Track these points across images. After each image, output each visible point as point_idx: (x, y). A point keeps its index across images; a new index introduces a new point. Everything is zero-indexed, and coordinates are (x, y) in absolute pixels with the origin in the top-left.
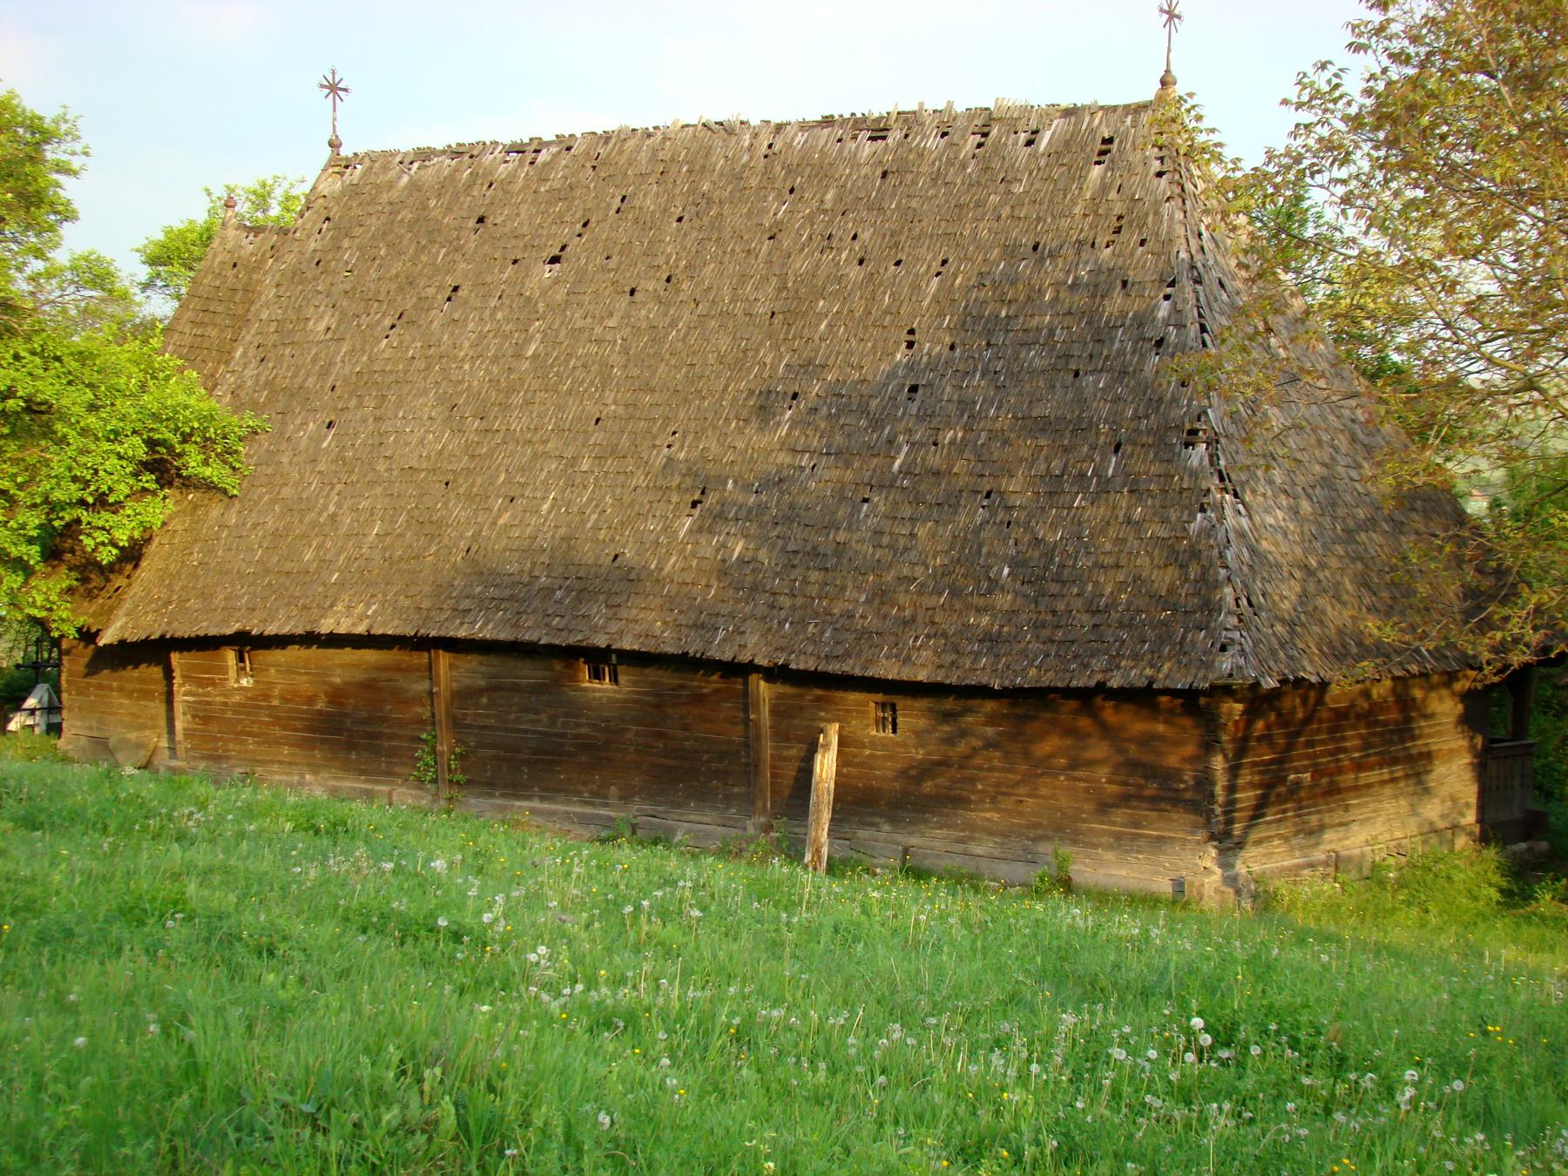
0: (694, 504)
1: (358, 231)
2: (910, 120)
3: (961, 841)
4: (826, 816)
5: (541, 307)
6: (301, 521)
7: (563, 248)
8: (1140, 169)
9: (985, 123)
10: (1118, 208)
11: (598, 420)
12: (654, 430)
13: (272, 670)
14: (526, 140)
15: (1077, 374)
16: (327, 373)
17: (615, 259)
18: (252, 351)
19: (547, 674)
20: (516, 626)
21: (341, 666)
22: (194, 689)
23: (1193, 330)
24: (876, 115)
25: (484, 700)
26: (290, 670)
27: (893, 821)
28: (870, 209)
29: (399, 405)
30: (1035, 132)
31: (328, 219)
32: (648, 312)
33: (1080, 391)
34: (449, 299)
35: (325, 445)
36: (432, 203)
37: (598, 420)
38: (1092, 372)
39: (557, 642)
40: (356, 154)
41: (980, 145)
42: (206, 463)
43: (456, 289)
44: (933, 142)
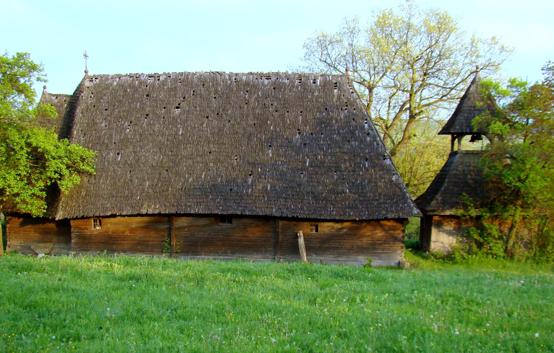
0: (250, 175)
1: (104, 97)
2: (277, 74)
3: (336, 257)
4: (305, 254)
5: (179, 121)
6: (119, 181)
7: (179, 104)
8: (347, 91)
9: (300, 77)
10: (345, 101)
11: (210, 153)
12: (230, 155)
13: (109, 225)
14: (153, 74)
15: (349, 141)
16: (112, 138)
17: (198, 109)
18: (80, 132)
19: (209, 222)
20: (209, 209)
21: (136, 222)
23: (375, 131)
24: (265, 73)
25: (186, 230)
26: (116, 224)
27: (316, 254)
28: (274, 97)
29: (141, 147)
32: (215, 123)
33: (352, 146)
34: (146, 118)
35: (119, 159)
36: (129, 90)
37: (210, 153)
38: (353, 141)
39: (223, 213)
40: (94, 75)
41: (300, 82)
42: (83, 165)
43: (147, 115)
44: (286, 81)
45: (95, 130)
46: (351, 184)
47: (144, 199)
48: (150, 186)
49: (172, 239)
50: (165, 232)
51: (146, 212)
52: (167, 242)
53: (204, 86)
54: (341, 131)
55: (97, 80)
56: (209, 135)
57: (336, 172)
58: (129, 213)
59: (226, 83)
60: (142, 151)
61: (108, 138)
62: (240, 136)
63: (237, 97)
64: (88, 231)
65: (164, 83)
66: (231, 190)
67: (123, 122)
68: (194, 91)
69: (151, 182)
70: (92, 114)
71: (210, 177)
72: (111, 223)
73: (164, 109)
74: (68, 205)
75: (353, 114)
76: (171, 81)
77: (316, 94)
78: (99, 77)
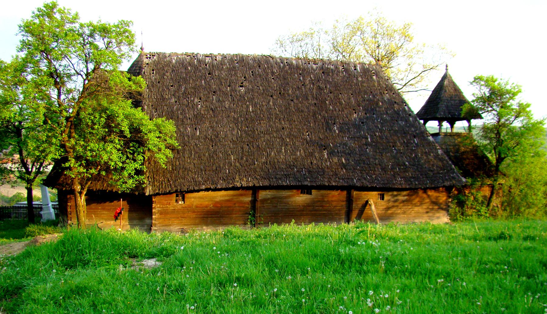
7: (242, 83)
10: (384, 86)
11: (283, 129)
14: (208, 54)
22: (162, 206)
25: (269, 201)
26: (200, 198)
30: (355, 67)
31: (153, 70)
32: (280, 101)
34: (214, 95)
37: (283, 129)
41: (343, 69)
43: (214, 92)
45: (166, 105)
46: (408, 158)
47: (233, 173)
48: (237, 160)
49: (257, 211)
50: (248, 204)
51: (241, 185)
52: (250, 214)
53: (261, 68)
54: (389, 112)
55: (155, 57)
56: (278, 113)
57: (393, 147)
58: (224, 186)
59: (280, 66)
60: (219, 126)
61: (181, 114)
62: (306, 114)
63: (293, 79)
64: (170, 206)
65: (222, 63)
66: (311, 163)
67: (192, 99)
68: (252, 72)
69: (235, 156)
70: (159, 90)
71: (290, 151)
72: (195, 198)
73: (229, 88)
74: (155, 180)
75: (394, 98)
76: (228, 62)
77: (360, 79)
78: (156, 54)
